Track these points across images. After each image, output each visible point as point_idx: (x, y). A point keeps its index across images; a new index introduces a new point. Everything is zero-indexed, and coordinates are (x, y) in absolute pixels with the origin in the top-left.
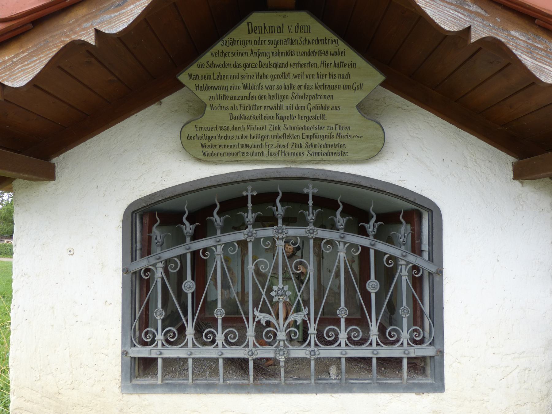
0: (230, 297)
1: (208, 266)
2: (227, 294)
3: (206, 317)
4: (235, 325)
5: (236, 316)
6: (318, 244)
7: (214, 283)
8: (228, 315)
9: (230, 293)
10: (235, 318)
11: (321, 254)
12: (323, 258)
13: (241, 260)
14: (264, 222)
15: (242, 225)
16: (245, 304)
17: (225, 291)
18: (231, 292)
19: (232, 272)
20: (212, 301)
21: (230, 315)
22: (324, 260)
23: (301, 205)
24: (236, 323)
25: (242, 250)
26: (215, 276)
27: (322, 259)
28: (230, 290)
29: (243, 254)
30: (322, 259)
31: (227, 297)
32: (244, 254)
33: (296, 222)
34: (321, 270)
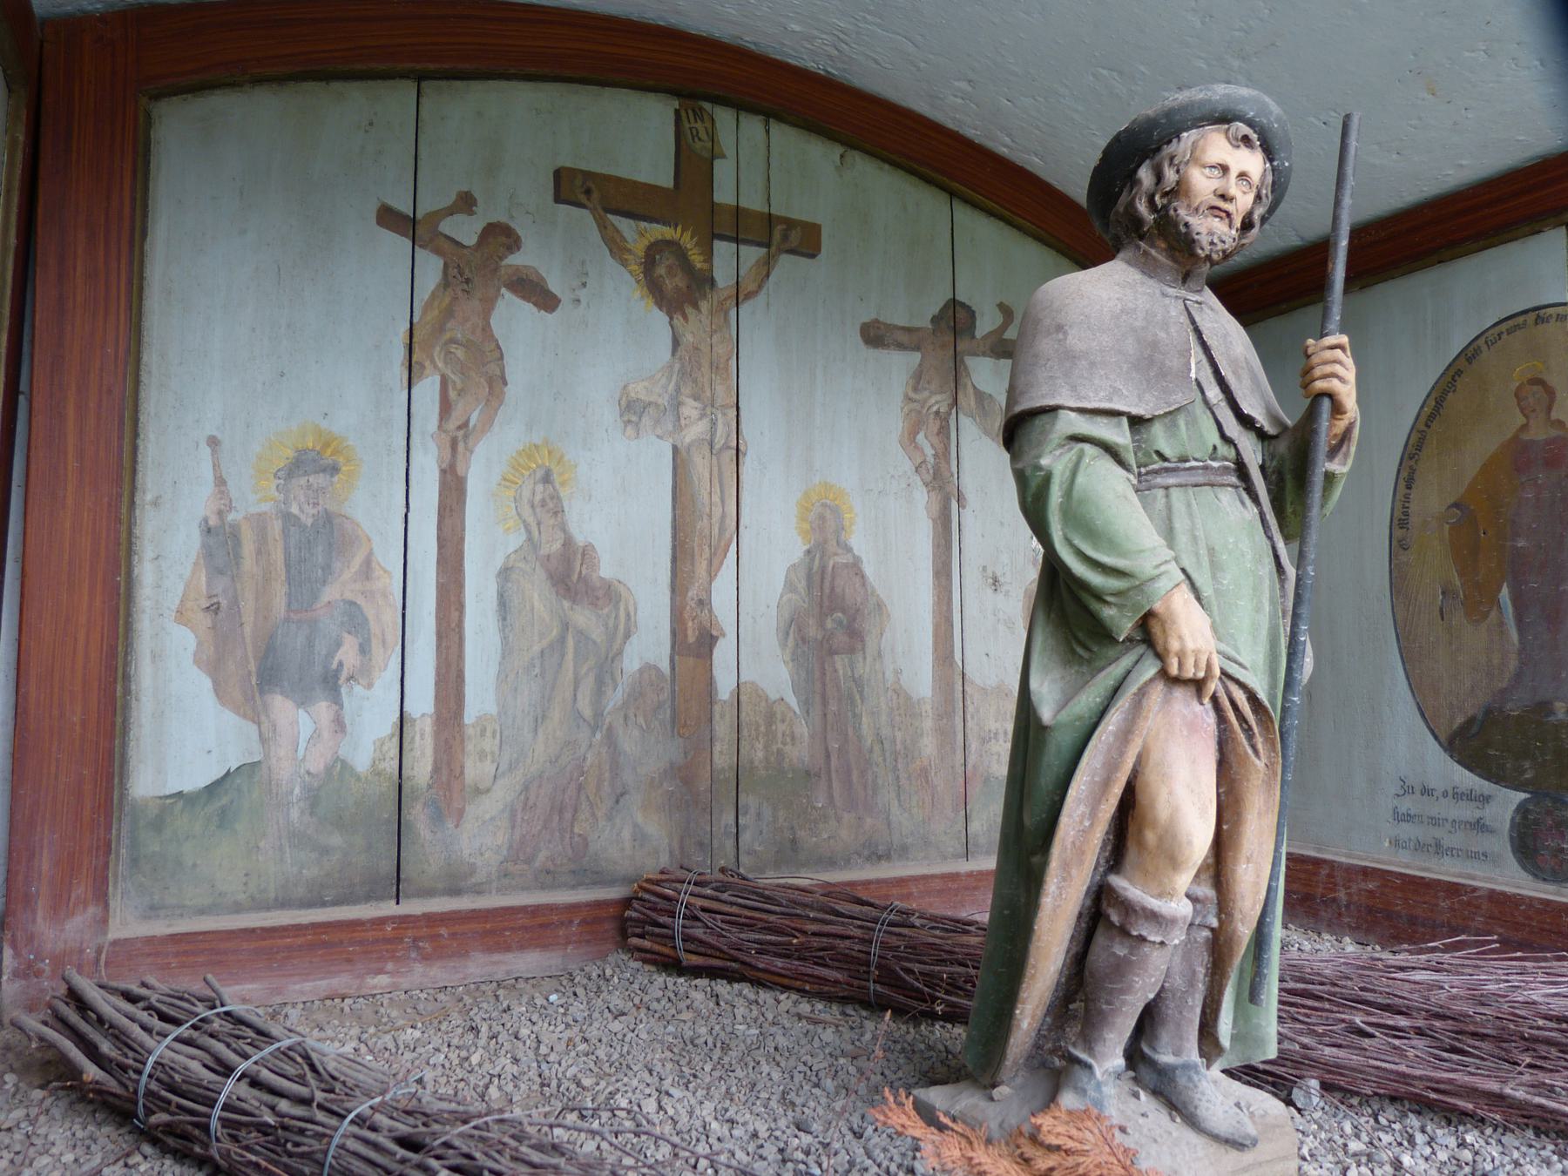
0: (344, 762)
1: (149, 497)
2: (316, 736)
3: (115, 943)
4: (383, 980)
5: (389, 908)
6: (937, 413)
7: (200, 644)
8: (324, 904)
9: (339, 725)
10: (380, 922)
11: (952, 475)
12: (960, 499)
13: (443, 472)
14: (610, 216)
15: (450, 211)
16: (461, 813)
17: (301, 711)
18: (347, 722)
19: (368, 562)
20: (180, 794)
21: (337, 903)
22: (966, 513)
23: (842, 156)
24: (390, 966)
25: (452, 394)
26: (209, 585)
27: (954, 505)
28: (342, 706)
29: (452, 425)
30: (954, 505)
31: (316, 764)
32: (465, 425)
33: (813, 256)
34: (949, 576)
